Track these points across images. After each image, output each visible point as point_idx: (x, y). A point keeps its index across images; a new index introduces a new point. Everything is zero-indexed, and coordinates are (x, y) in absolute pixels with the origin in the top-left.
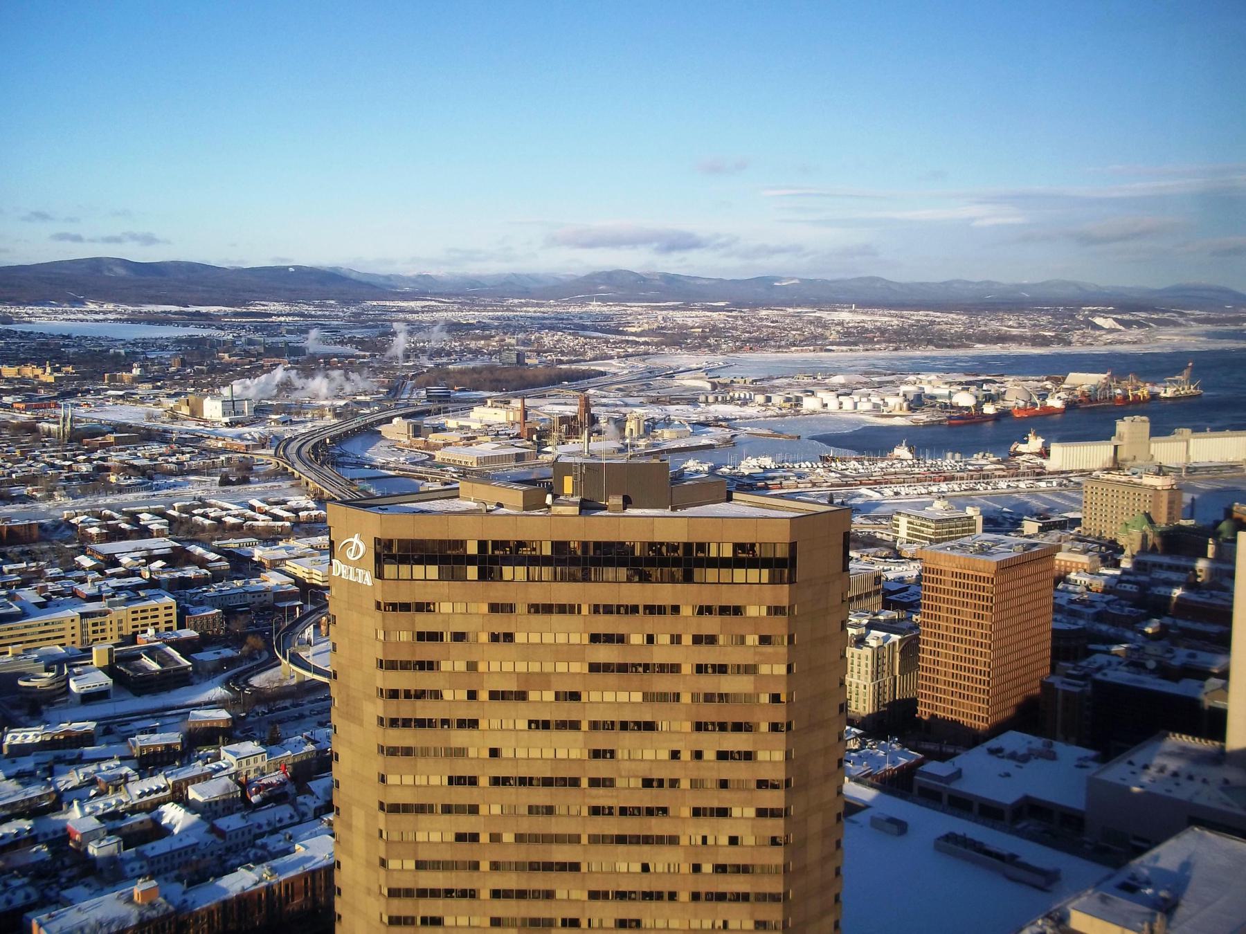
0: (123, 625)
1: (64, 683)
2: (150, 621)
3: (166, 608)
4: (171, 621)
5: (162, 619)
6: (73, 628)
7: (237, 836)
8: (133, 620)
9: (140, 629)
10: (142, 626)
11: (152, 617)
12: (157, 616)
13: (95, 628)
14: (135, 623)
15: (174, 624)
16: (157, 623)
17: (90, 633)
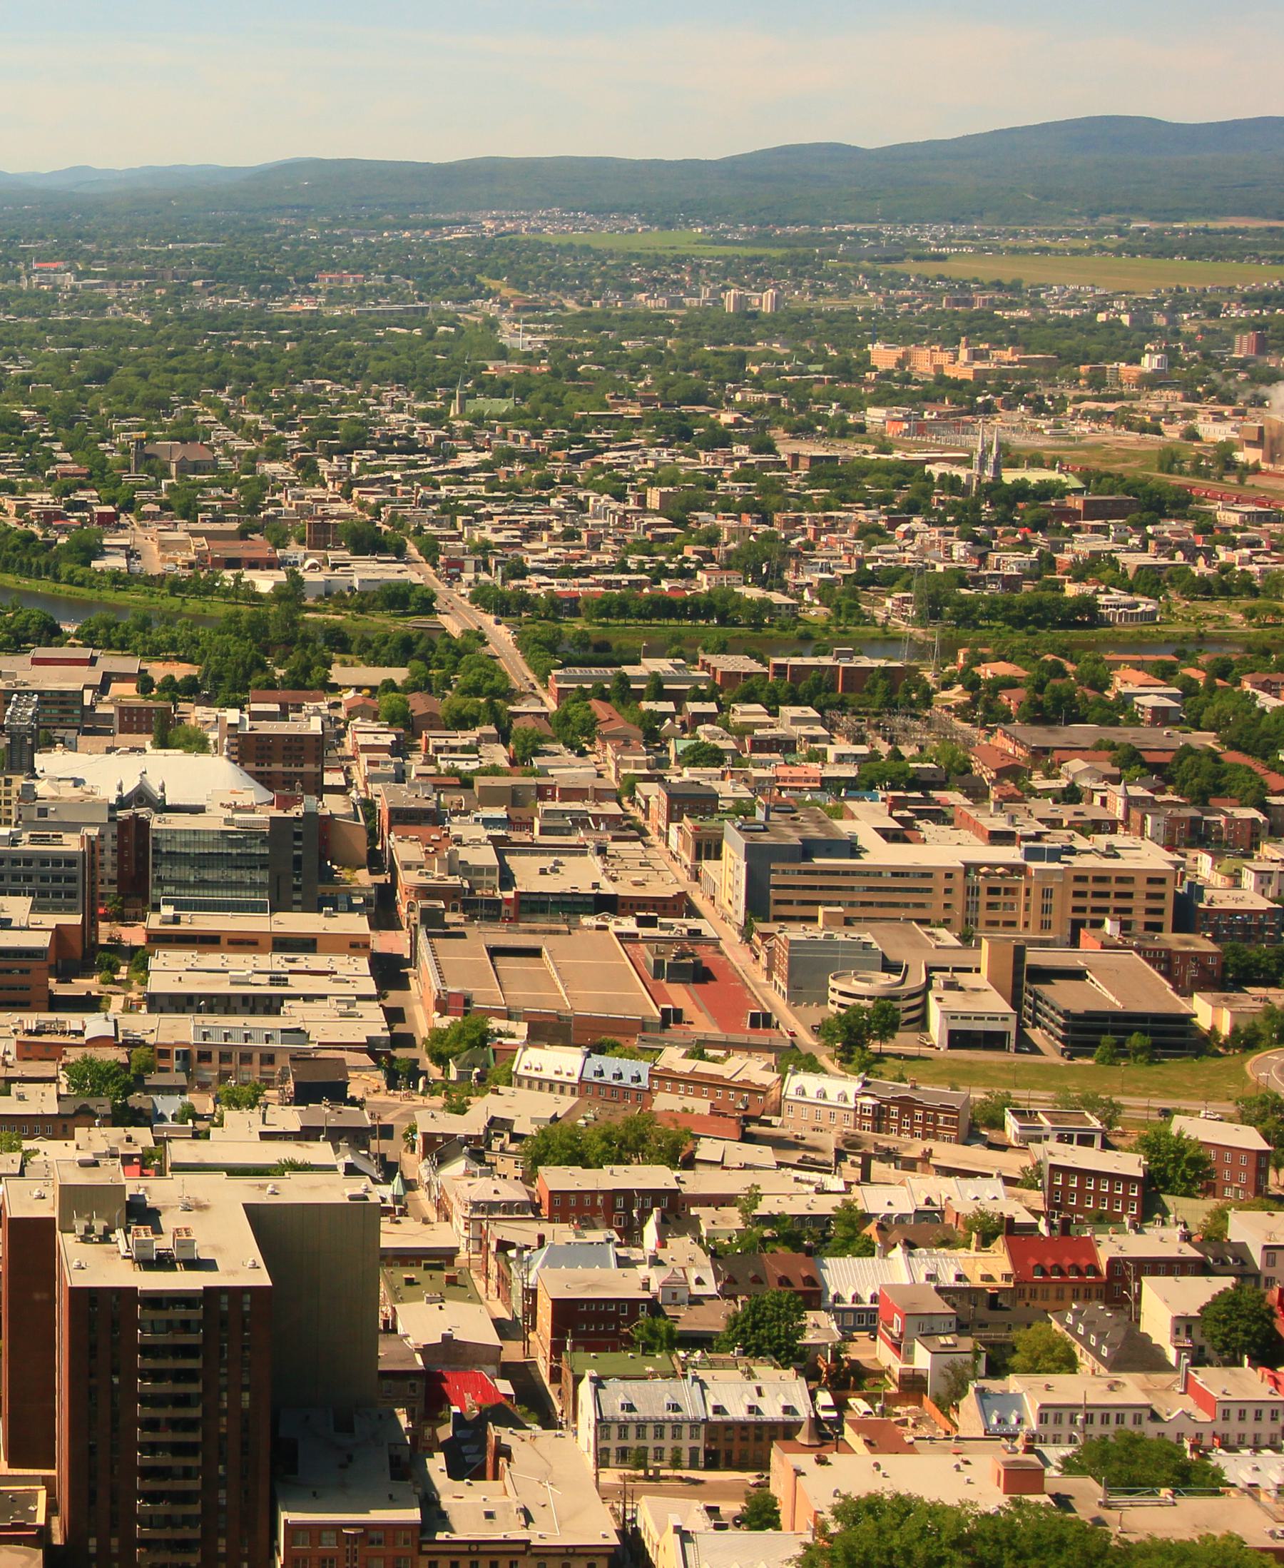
0: (1055, 902)
1: (917, 1001)
2: (1112, 903)
3: (1150, 881)
4: (1160, 912)
5: (1139, 904)
6: (948, 891)
7: (1242, 1415)
8: (1077, 894)
9: (1089, 916)
10: (1095, 910)
11: (1118, 895)
12: (1129, 895)
13: (993, 898)
14: (1080, 902)
15: (1167, 919)
16: (1128, 911)
17: (983, 906)
